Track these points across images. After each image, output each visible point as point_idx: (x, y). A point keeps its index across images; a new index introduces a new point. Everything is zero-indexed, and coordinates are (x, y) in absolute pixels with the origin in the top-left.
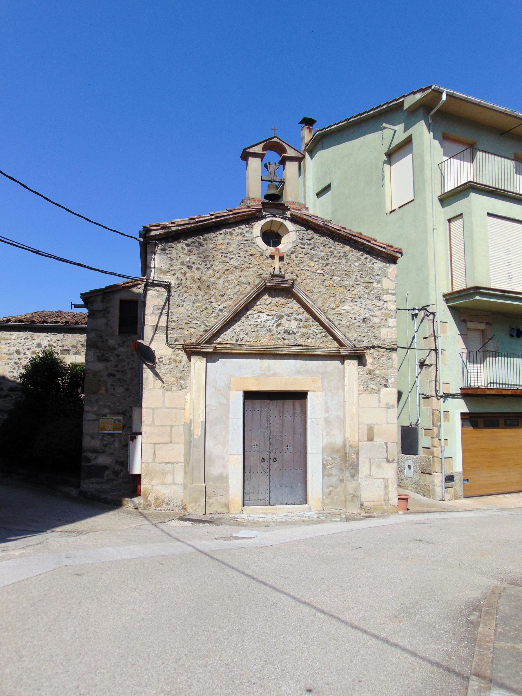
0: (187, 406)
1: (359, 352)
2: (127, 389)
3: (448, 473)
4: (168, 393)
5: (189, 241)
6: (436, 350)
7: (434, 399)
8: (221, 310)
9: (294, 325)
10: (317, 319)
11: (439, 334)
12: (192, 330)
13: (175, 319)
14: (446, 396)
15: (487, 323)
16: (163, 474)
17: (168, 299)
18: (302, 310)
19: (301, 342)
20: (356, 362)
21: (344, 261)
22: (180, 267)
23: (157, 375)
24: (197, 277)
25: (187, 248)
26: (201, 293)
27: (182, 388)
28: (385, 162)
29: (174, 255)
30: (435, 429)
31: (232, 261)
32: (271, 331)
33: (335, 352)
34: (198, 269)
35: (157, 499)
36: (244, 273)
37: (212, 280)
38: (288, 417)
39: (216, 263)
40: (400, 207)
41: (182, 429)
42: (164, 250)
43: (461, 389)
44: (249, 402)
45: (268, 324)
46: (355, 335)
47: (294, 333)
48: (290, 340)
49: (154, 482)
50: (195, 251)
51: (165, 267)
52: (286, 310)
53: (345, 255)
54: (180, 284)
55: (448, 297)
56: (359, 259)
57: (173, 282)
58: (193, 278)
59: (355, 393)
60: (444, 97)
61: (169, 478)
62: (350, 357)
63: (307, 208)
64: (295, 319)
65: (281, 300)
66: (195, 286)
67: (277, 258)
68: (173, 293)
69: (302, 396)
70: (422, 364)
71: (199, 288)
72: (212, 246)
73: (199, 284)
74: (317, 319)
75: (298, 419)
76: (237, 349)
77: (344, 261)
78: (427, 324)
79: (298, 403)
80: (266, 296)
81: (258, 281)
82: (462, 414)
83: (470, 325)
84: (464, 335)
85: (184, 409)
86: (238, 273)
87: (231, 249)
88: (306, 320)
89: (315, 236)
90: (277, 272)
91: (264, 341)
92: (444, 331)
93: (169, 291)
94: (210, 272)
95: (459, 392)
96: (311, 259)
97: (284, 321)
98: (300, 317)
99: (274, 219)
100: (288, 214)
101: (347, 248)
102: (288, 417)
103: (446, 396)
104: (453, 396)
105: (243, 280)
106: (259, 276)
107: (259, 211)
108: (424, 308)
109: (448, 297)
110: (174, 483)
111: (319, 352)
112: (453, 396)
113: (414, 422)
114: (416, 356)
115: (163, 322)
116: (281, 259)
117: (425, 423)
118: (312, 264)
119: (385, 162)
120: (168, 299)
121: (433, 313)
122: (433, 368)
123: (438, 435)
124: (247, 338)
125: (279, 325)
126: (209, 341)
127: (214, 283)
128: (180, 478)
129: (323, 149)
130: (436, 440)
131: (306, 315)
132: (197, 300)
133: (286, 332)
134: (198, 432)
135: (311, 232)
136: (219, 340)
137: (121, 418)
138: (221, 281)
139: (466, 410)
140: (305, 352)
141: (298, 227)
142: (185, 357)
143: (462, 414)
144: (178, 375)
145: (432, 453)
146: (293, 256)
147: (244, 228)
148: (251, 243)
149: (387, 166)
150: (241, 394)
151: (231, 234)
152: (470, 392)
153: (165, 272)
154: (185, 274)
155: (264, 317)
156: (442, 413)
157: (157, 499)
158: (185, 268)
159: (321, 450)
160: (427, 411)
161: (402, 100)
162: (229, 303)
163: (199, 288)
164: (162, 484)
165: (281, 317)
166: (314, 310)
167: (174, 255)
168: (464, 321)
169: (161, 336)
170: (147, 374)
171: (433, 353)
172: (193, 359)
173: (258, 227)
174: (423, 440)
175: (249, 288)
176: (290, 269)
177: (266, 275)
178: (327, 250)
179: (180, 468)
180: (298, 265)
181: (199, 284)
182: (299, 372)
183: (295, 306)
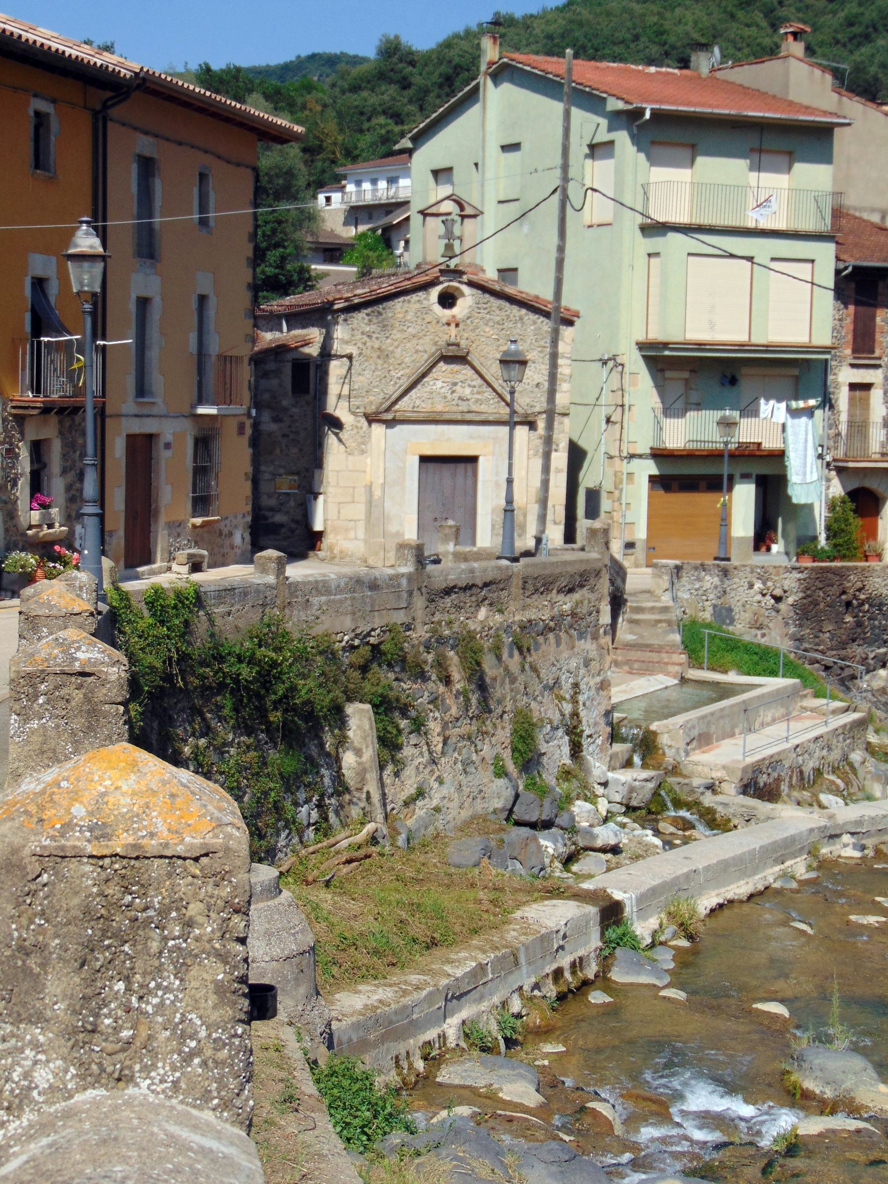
0: (368, 469)
1: (529, 419)
2: (301, 450)
3: (629, 539)
4: (350, 458)
5: (369, 310)
6: (622, 406)
7: (617, 460)
8: (399, 378)
9: (468, 391)
10: (489, 385)
11: (626, 387)
12: (372, 398)
13: (356, 387)
14: (632, 456)
15: (691, 371)
16: (347, 530)
17: (350, 368)
18: (476, 376)
19: (474, 408)
20: (526, 428)
21: (519, 325)
22: (360, 336)
23: (340, 440)
24: (376, 346)
25: (367, 318)
26: (380, 362)
27: (363, 452)
28: (587, 156)
29: (355, 326)
30: (617, 493)
31: (410, 330)
32: (445, 397)
33: (506, 418)
34: (377, 338)
35: (341, 552)
36: (421, 341)
37: (391, 349)
38: (460, 479)
39: (395, 332)
40: (599, 225)
41: (363, 490)
42: (345, 320)
43: (651, 448)
44: (425, 465)
45: (443, 390)
46: (528, 400)
47: (468, 400)
48: (464, 407)
49: (339, 537)
50: (375, 321)
51: (347, 337)
52: (461, 377)
53: (521, 319)
54: (361, 354)
55: (642, 346)
56: (535, 323)
57: (355, 352)
58: (372, 348)
59: (525, 458)
60: (648, 115)
61: (352, 534)
62: (522, 423)
63: (483, 271)
64: (469, 386)
65: (455, 367)
66: (375, 355)
67: (453, 325)
68: (354, 363)
69: (472, 460)
70: (608, 421)
71: (379, 357)
72: (390, 315)
73: (378, 353)
74: (489, 385)
75: (469, 482)
76: (414, 416)
77: (519, 325)
78: (615, 375)
79: (469, 466)
80: (441, 364)
81: (434, 349)
82: (651, 477)
83: (668, 374)
84: (660, 387)
85: (365, 472)
86: (415, 341)
87: (409, 317)
88: (480, 386)
89: (492, 299)
90: (453, 340)
91: (439, 408)
92: (634, 384)
93: (351, 361)
94: (389, 341)
95: (648, 451)
96: (486, 324)
97: (458, 388)
98: (474, 383)
99: (451, 284)
100: (465, 278)
101: (524, 311)
102: (460, 479)
103: (632, 456)
104: (640, 456)
105: (420, 348)
106: (436, 343)
107: (437, 278)
108: (613, 358)
109: (642, 346)
110: (356, 539)
111: (491, 418)
112: (640, 456)
113: (597, 483)
114: (604, 412)
115: (345, 391)
116: (457, 325)
117: (607, 486)
118: (487, 329)
119: (587, 156)
120: (350, 368)
121: (622, 365)
122: (618, 426)
123: (619, 499)
124: (423, 405)
125: (453, 392)
126: (388, 410)
127: (392, 352)
128: (361, 534)
129: (512, 81)
130: (616, 504)
131: (479, 381)
132: (376, 369)
133: (460, 398)
134: (377, 493)
135: (487, 296)
136: (397, 407)
137: (296, 478)
138: (399, 350)
139: (655, 471)
140: (478, 418)
141: (474, 291)
142: (366, 424)
143: (651, 477)
144: (360, 440)
145: (612, 518)
146: (469, 321)
147: (421, 294)
148: (428, 310)
149: (589, 162)
150: (416, 459)
151: (409, 302)
152: (658, 452)
153: (347, 343)
154: (365, 344)
155: (439, 384)
156: (625, 476)
157: (341, 552)
158: (365, 338)
159: (490, 511)
160: (610, 472)
161: (604, 95)
162: (407, 371)
163: (379, 357)
164: (345, 539)
165: (455, 384)
166: (488, 377)
167: (355, 326)
168: (662, 370)
169: (344, 404)
170: (331, 440)
171: (619, 409)
172: (374, 426)
173: (435, 292)
174: (605, 504)
175: (426, 356)
176: (466, 335)
177: (442, 343)
178: (504, 313)
179: (361, 525)
180: (473, 330)
181: (378, 353)
182: (471, 437)
183: (467, 372)
